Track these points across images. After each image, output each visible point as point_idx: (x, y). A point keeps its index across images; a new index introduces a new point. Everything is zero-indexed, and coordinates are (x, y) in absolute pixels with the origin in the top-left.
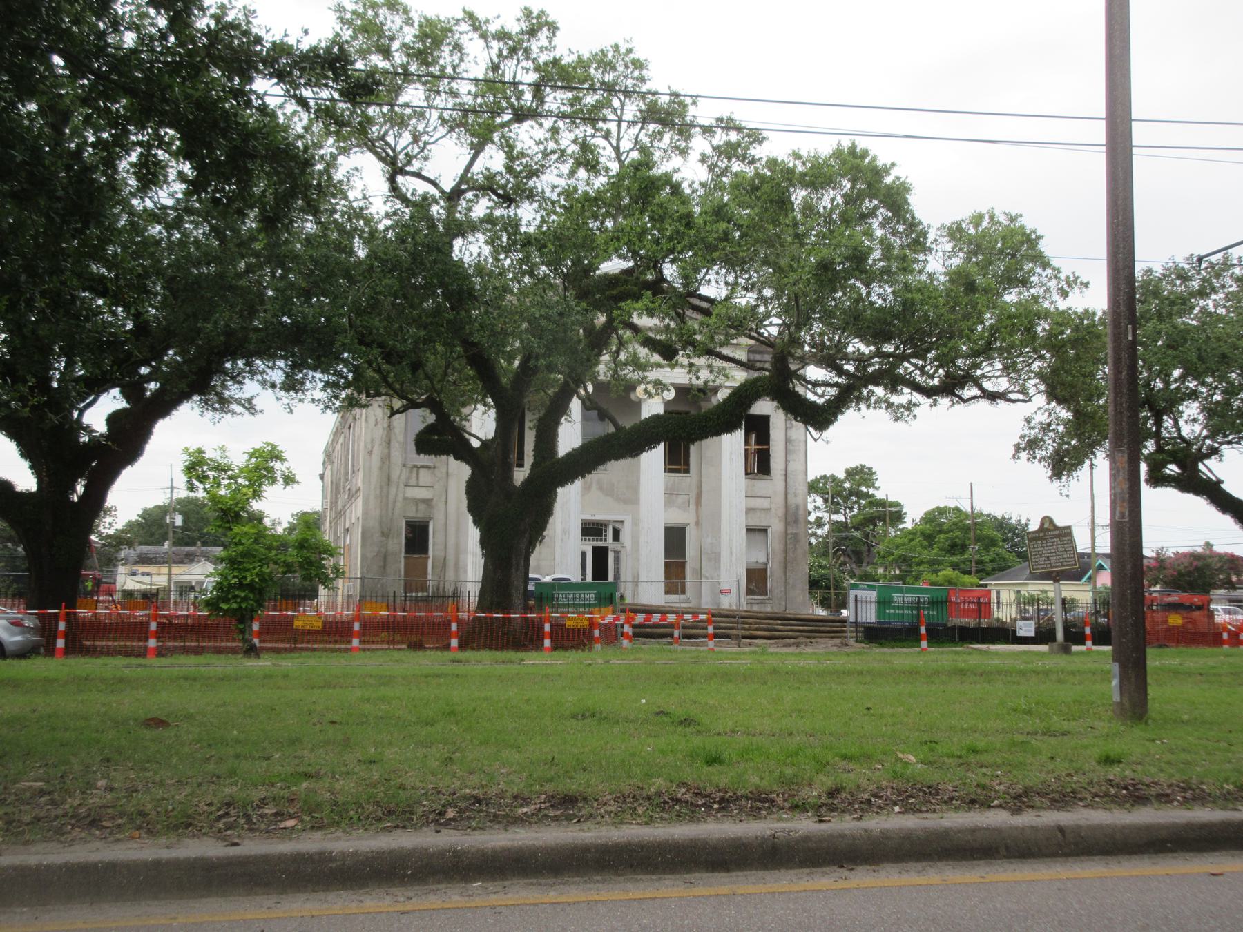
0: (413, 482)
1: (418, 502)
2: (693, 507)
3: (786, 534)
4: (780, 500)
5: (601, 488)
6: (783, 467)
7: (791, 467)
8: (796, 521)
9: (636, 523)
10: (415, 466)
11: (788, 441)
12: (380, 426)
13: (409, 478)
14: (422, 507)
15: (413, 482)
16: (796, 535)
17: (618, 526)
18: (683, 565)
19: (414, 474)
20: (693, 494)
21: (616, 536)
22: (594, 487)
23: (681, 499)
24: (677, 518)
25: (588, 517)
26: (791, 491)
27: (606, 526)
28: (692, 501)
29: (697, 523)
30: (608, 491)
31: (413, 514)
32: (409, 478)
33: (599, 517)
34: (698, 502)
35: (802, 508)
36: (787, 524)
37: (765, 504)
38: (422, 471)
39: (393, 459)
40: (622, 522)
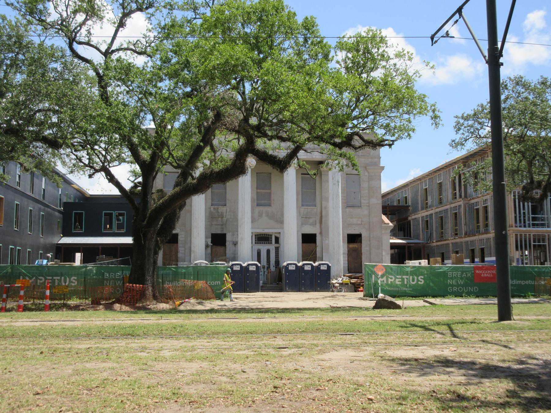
2: (318, 225)
5: (267, 216)
9: (284, 232)
17: (277, 235)
20: (318, 218)
21: (277, 240)
22: (264, 215)
23: (311, 221)
24: (309, 230)
25: (260, 231)
27: (271, 235)
28: (318, 221)
29: (321, 233)
30: (272, 217)
33: (267, 231)
40: (280, 233)
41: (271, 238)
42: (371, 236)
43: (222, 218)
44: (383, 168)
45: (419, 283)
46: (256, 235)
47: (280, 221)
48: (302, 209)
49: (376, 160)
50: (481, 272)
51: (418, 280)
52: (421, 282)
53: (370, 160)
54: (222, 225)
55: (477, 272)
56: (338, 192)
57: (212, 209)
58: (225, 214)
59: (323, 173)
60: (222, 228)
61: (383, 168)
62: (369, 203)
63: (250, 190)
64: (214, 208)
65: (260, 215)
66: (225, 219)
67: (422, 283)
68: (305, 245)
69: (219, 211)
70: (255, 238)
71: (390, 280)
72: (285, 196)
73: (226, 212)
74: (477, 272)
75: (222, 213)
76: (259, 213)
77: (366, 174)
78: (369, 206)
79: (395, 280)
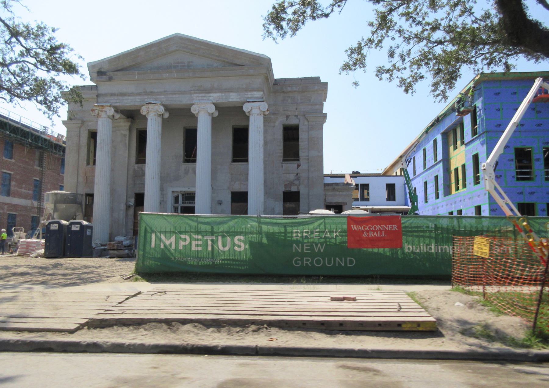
42: (310, 194)
45: (236, 248)
46: (183, 195)
49: (317, 107)
50: (362, 228)
51: (234, 245)
52: (239, 246)
53: (310, 107)
55: (354, 227)
57: (136, 167)
62: (308, 156)
64: (138, 167)
67: (242, 249)
68: (234, 204)
70: (183, 198)
71: (182, 243)
74: (354, 227)
76: (185, 170)
77: (306, 123)
78: (308, 159)
79: (190, 244)
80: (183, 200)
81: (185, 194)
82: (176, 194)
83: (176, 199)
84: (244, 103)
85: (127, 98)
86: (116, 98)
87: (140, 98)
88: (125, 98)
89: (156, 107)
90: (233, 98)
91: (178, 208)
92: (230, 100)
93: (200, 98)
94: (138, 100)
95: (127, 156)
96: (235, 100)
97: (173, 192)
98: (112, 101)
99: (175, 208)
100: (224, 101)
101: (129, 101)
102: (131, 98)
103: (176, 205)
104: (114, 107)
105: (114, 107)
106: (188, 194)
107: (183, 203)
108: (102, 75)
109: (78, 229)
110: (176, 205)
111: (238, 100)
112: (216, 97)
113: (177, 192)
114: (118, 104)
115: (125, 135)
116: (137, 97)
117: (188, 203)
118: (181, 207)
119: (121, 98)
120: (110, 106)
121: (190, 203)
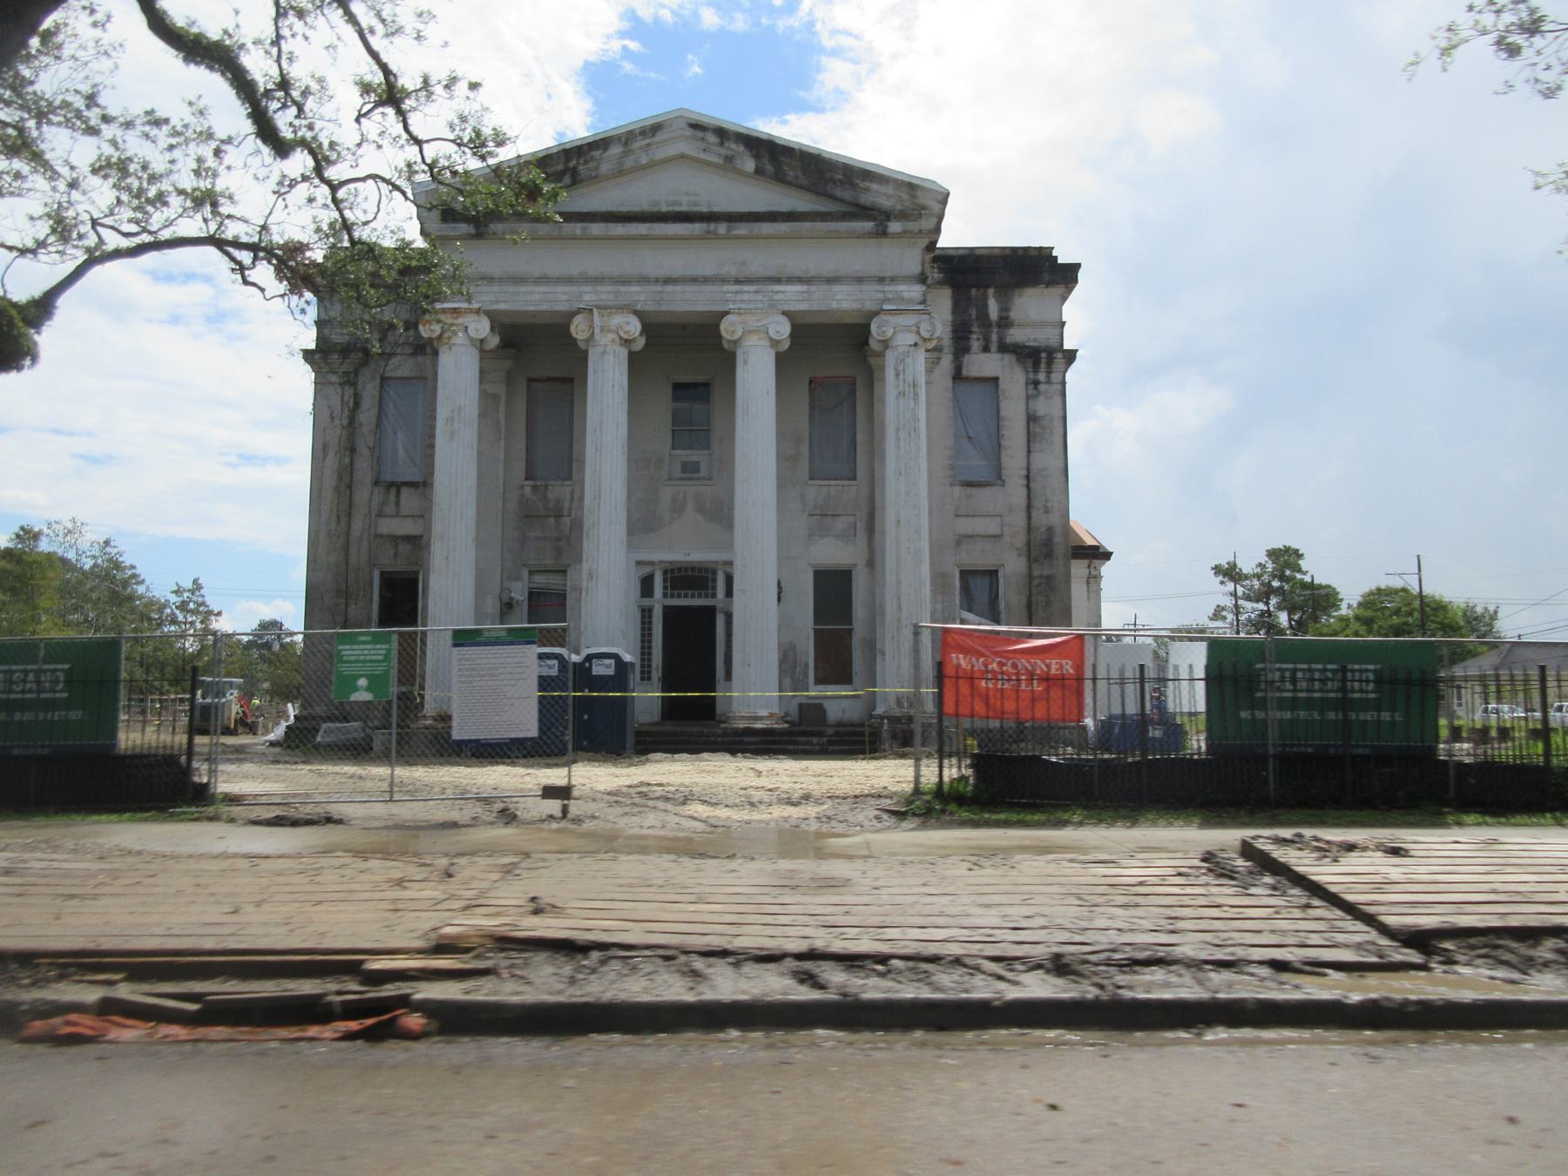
0: (390, 509)
1: (395, 539)
2: (861, 536)
3: (1030, 576)
4: (1019, 519)
5: (700, 509)
6: (1024, 464)
7: (1039, 460)
8: (1049, 555)
10: (392, 484)
11: (1032, 418)
12: (337, 422)
13: (384, 503)
14: (405, 548)
15: (390, 509)
16: (1049, 579)
18: (850, 631)
19: (392, 497)
22: (690, 507)
23: (840, 524)
24: (833, 553)
26: (1038, 503)
27: (714, 572)
31: (391, 561)
32: (384, 503)
33: (698, 556)
34: (871, 528)
35: (1059, 531)
36: (1031, 560)
37: (992, 527)
38: (405, 492)
39: (358, 475)
41: (714, 580)
43: (559, 516)
44: (1071, 356)
46: (665, 572)
47: (721, 515)
48: (816, 492)
54: (559, 539)
56: (916, 420)
57: (528, 490)
58: (566, 505)
59: (876, 374)
60: (559, 552)
61: (1071, 356)
63: (622, 417)
64: (534, 488)
65: (678, 508)
66: (566, 520)
69: (550, 495)
70: (665, 580)
72: (738, 435)
73: (572, 499)
75: (558, 501)
76: (674, 500)
80: (665, 588)
81: (673, 571)
82: (646, 570)
83: (646, 586)
84: (876, 313)
85: (530, 288)
86: (495, 289)
87: (567, 289)
88: (523, 289)
89: (617, 320)
90: (843, 301)
91: (650, 610)
92: (834, 305)
93: (746, 297)
94: (564, 297)
95: (502, 456)
96: (846, 306)
97: (639, 563)
98: (485, 298)
99: (643, 610)
100: (815, 307)
101: (537, 297)
102: (542, 289)
103: (647, 602)
104: (491, 315)
105: (488, 314)
106: (679, 569)
107: (665, 596)
108: (455, 220)
109: (611, 672)
110: (647, 602)
111: (856, 306)
112: (793, 296)
113: (652, 563)
114: (502, 306)
115: (495, 397)
116: (560, 289)
117: (679, 596)
118: (665, 608)
119: (511, 288)
120: (478, 311)
121: (686, 596)
